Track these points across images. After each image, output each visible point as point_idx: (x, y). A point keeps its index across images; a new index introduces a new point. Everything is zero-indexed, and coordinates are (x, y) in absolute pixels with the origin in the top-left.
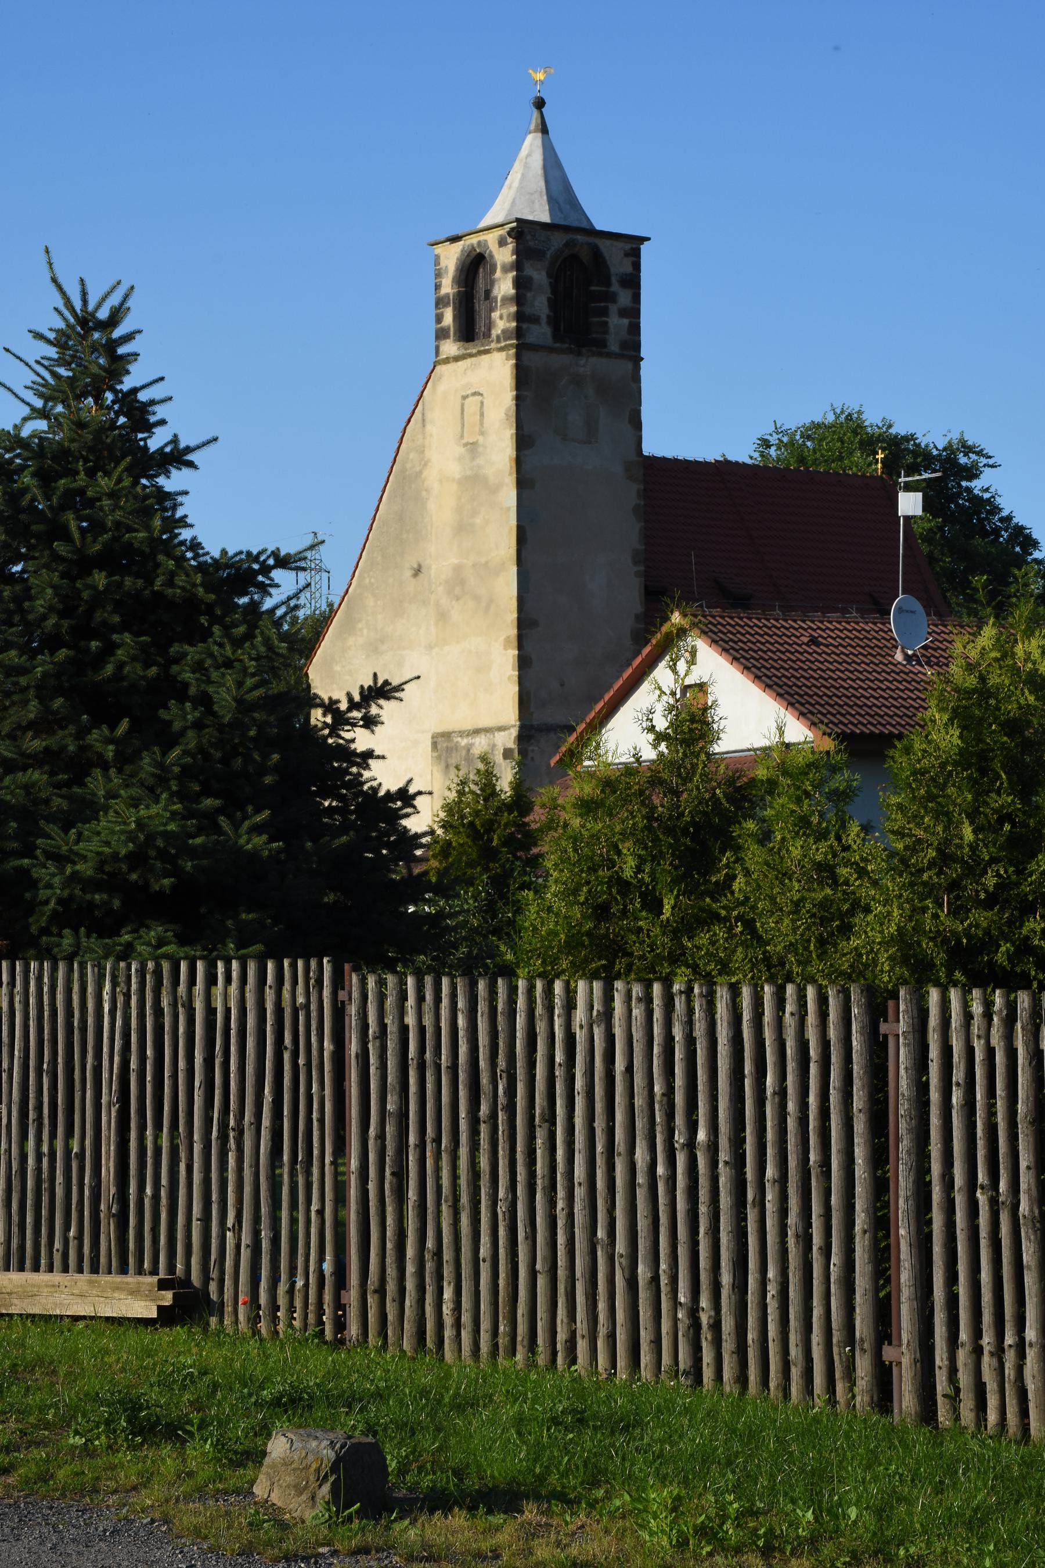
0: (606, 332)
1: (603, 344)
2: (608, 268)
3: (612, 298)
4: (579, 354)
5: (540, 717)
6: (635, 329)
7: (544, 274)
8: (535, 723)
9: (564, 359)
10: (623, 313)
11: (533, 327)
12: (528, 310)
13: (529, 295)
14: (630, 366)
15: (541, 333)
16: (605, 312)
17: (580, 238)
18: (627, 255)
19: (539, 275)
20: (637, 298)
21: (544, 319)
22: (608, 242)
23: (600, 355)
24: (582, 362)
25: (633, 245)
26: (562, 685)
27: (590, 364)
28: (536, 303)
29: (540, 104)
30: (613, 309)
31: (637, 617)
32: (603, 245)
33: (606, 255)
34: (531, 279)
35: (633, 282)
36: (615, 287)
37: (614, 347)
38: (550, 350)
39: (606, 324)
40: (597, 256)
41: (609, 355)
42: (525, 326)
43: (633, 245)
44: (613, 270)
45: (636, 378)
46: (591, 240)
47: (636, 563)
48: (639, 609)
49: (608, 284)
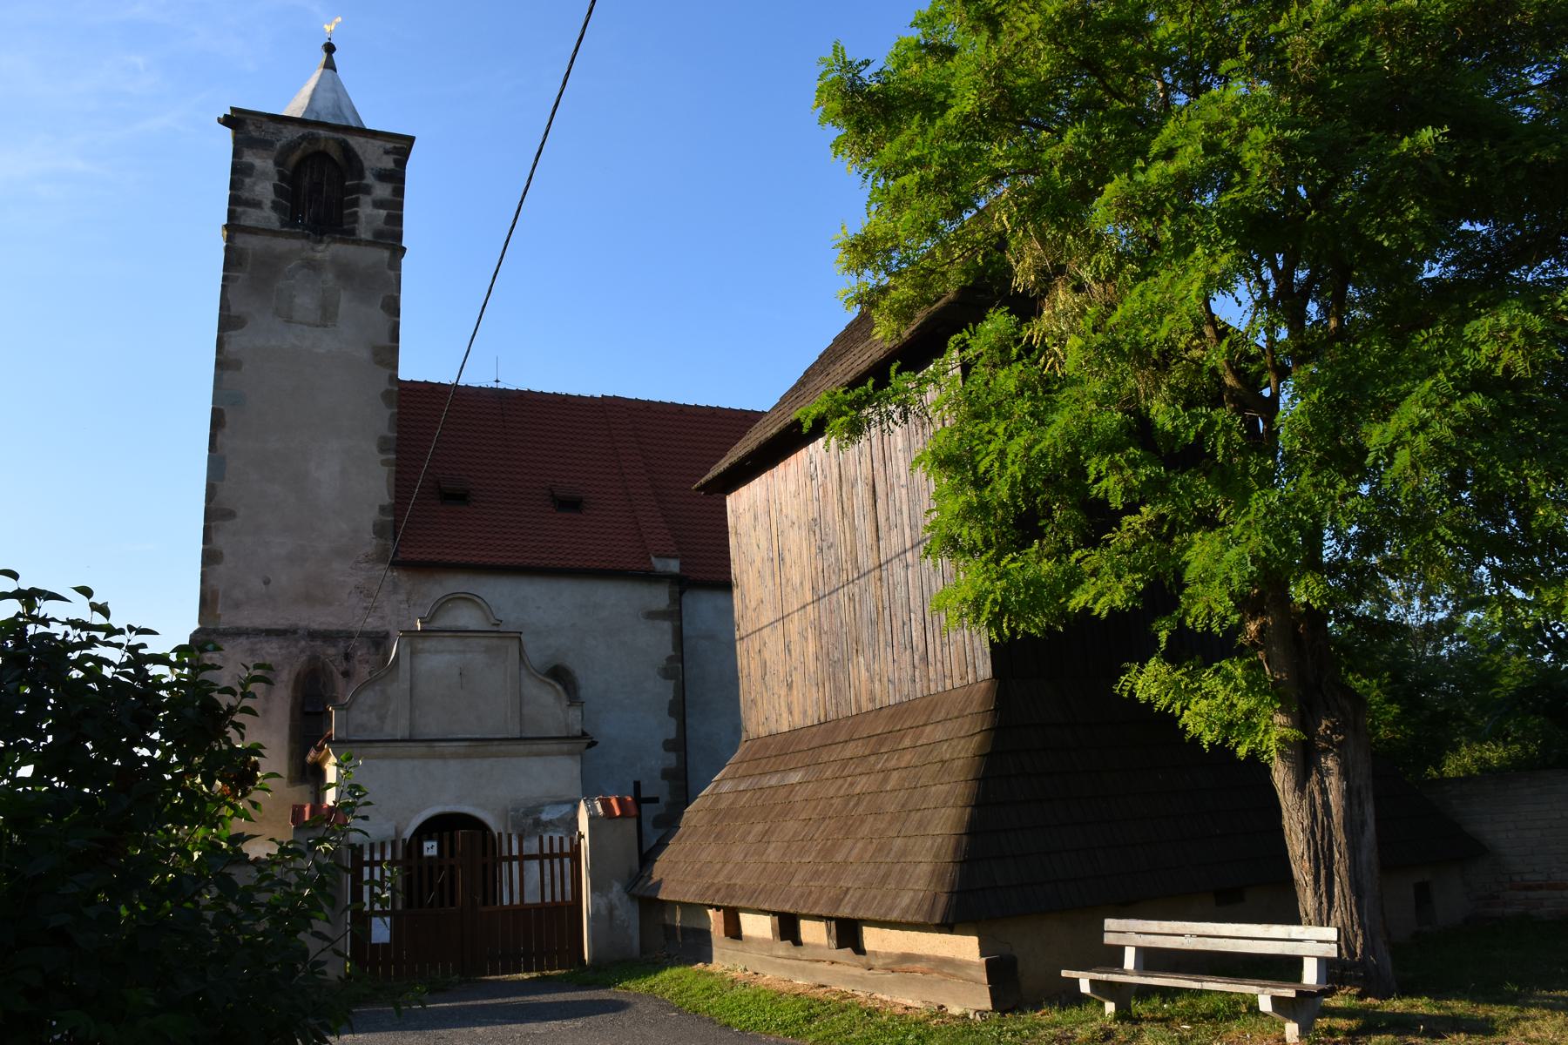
0: (356, 221)
1: (352, 232)
2: (360, 162)
3: (367, 190)
4: (321, 242)
5: (227, 619)
6: (396, 220)
7: (270, 163)
8: (221, 627)
9: (296, 244)
10: (379, 204)
11: (250, 210)
12: (245, 194)
13: (247, 181)
14: (386, 254)
15: (267, 216)
16: (355, 203)
17: (322, 133)
18: (387, 152)
19: (263, 163)
20: (399, 191)
21: (268, 204)
22: (362, 140)
23: (344, 241)
24: (321, 247)
25: (401, 146)
26: (267, 582)
27: (328, 251)
28: (258, 188)
29: (330, 48)
30: (366, 200)
31: (382, 509)
32: (355, 142)
33: (360, 152)
34: (251, 167)
35: (396, 178)
36: (369, 179)
37: (364, 233)
38: (274, 233)
39: (356, 213)
40: (347, 150)
41: (358, 242)
42: (239, 209)
43: (401, 146)
44: (366, 164)
45: (395, 266)
46: (340, 136)
47: (382, 451)
48: (387, 500)
49: (361, 175)
